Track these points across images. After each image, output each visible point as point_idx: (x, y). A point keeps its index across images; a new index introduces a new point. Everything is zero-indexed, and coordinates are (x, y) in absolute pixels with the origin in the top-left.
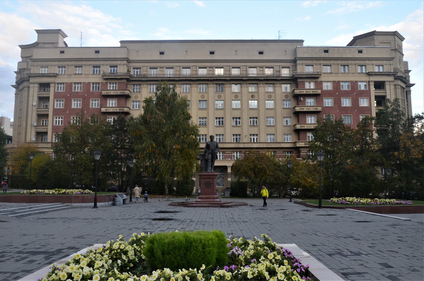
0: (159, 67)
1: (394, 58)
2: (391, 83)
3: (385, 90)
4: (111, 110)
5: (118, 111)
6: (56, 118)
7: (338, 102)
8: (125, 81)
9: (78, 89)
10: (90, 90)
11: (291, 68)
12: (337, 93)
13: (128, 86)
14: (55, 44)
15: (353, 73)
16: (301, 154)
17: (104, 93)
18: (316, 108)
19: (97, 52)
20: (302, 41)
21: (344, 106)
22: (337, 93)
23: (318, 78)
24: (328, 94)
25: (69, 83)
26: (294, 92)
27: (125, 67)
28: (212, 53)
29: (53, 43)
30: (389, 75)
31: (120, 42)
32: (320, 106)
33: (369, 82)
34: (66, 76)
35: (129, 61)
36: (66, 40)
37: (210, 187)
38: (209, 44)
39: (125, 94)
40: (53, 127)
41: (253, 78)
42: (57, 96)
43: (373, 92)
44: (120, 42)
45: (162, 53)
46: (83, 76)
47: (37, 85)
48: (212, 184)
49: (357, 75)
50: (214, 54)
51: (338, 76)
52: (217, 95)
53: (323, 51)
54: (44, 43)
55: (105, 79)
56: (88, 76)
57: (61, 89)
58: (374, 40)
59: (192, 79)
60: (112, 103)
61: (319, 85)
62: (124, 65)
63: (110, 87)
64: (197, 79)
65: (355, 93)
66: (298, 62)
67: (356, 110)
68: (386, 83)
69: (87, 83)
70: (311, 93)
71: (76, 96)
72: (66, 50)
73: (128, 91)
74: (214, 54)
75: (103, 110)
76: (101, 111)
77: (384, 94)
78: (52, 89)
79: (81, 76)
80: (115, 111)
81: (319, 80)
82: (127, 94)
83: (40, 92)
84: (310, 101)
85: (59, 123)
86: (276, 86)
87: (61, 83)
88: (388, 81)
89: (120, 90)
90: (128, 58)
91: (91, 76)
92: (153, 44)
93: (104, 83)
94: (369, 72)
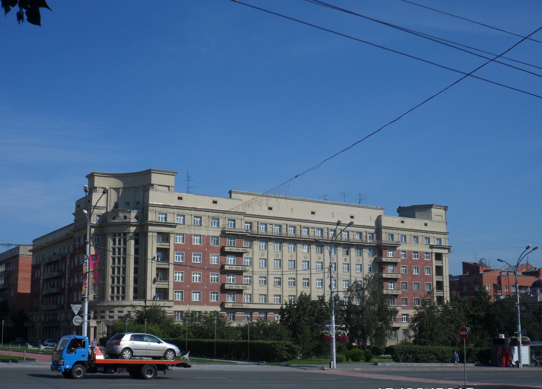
1: (449, 233)
2: (447, 255)
5: (234, 269)
18: (397, 275)
30: (445, 248)
40: (174, 283)
42: (177, 248)
43: (435, 263)
47: (156, 234)
49: (424, 245)
54: (159, 185)
58: (432, 212)
64: (304, 239)
69: (206, 236)
71: (196, 249)
78: (172, 240)
81: (398, 248)
83: (163, 243)
84: (390, 268)
87: (180, 234)
91: (210, 228)
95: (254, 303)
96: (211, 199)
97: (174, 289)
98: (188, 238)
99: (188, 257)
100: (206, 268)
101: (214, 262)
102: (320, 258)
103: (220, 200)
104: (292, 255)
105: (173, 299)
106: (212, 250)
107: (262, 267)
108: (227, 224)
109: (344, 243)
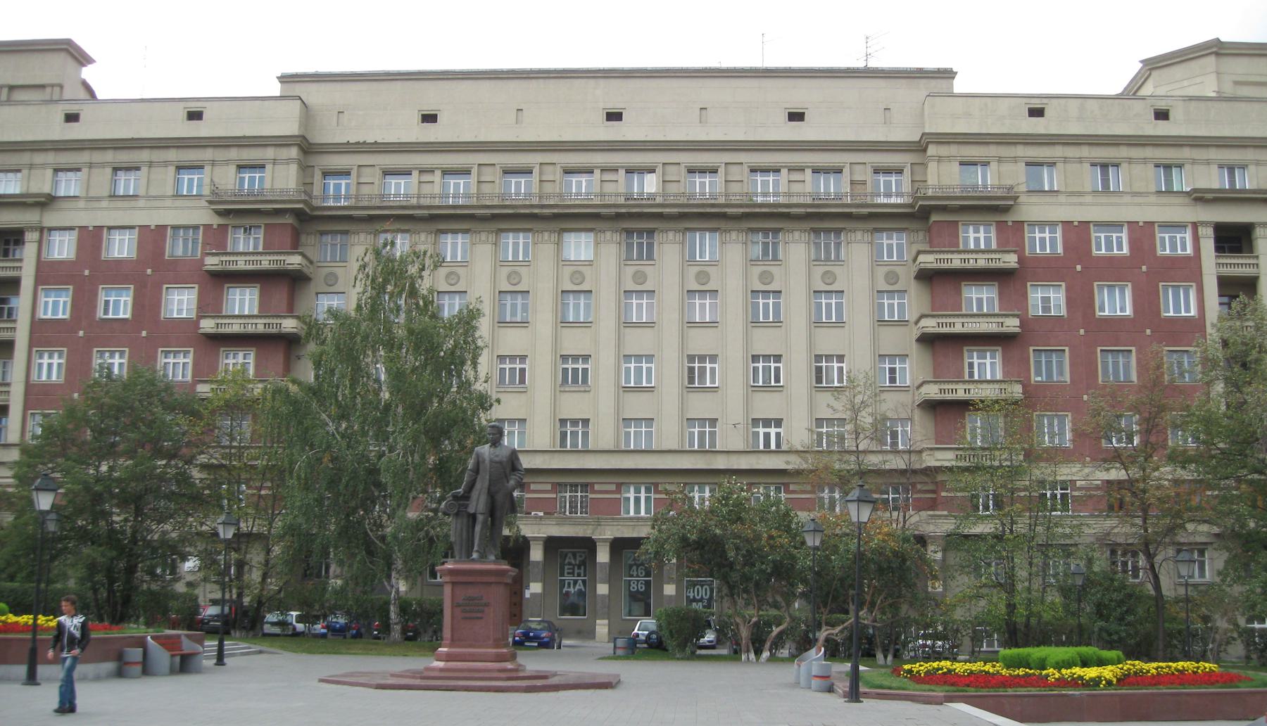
0: (416, 169)
3: (1254, 257)
4: (236, 328)
7: (1081, 301)
8: (289, 220)
9: (121, 247)
10: (163, 254)
11: (907, 171)
12: (1079, 268)
13: (303, 238)
14: (48, 90)
17: (212, 262)
18: (1000, 320)
19: (195, 116)
20: (948, 74)
21: (1106, 313)
22: (1079, 268)
23: (1006, 210)
24: (1047, 270)
25: (91, 228)
26: (917, 262)
27: (294, 168)
28: (614, 116)
29: (42, 87)
31: (278, 78)
32: (1014, 316)
33: (1195, 226)
35: (307, 148)
36: (87, 73)
37: (478, 618)
38: (602, 82)
39: (290, 267)
40: (29, 387)
41: (764, 210)
42: (49, 274)
43: (1211, 265)
44: (278, 78)
45: (429, 118)
46: (141, 203)
48: (458, 605)
49: (1153, 199)
50: (621, 120)
51: (1081, 204)
52: (630, 271)
54: (12, 88)
55: (221, 213)
57: (63, 248)
59: (536, 211)
60: (242, 302)
61: (1012, 233)
62: (289, 161)
63: (235, 240)
64: (555, 211)
65: (1144, 268)
66: (932, 150)
67: (1148, 332)
70: (982, 264)
71: (117, 273)
72: (86, 112)
73: (300, 257)
74: (621, 120)
75: (208, 325)
76: (201, 331)
78: (29, 252)
79: (133, 204)
80: (250, 329)
81: (1010, 218)
82: (297, 267)
84: (980, 296)
86: (853, 239)
89: (270, 254)
90: (304, 137)
91: (168, 203)
92: (399, 84)
93: (215, 227)
94: (1195, 191)
98: (91, 238)
101: (180, 311)
106: (178, 273)
109: (742, 210)
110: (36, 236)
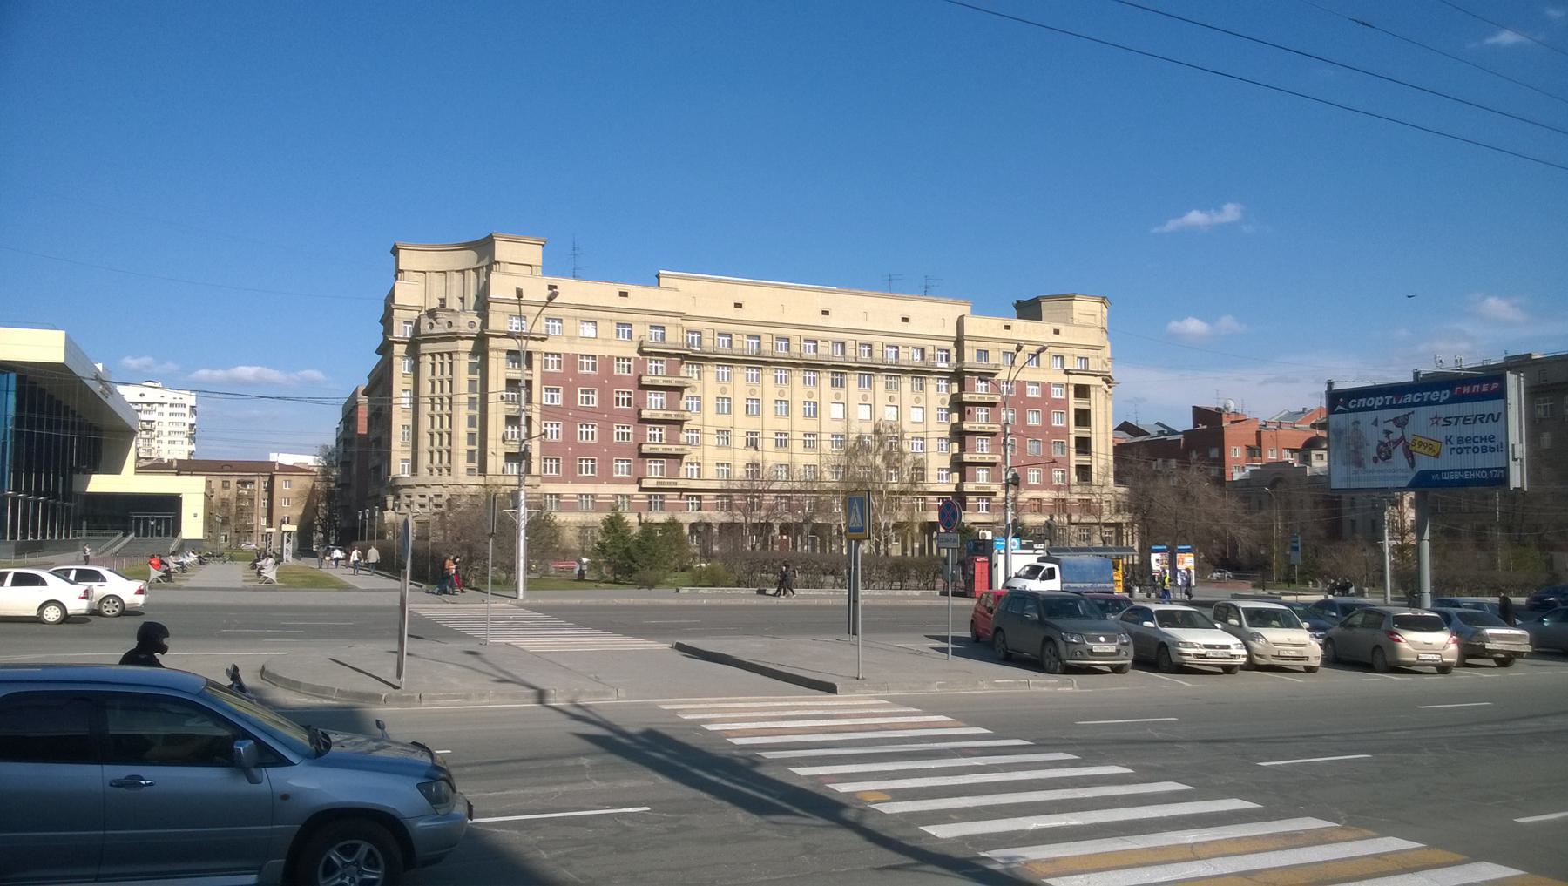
6: (581, 426)
15: (1045, 369)
16: (968, 503)
23: (993, 375)
33: (1067, 384)
34: (565, 340)
43: (1074, 403)
46: (599, 342)
47: (504, 354)
53: (1003, 327)
56: (609, 343)
58: (1072, 308)
68: (1091, 388)
77: (1087, 407)
78: (536, 364)
81: (996, 377)
84: (981, 413)
85: (587, 438)
88: (1093, 386)
91: (614, 343)
95: (707, 478)
96: (616, 288)
97: (541, 454)
98: (571, 361)
99: (570, 397)
100: (603, 416)
102: (840, 396)
103: (631, 289)
104: (752, 389)
105: (540, 472)
107: (723, 413)
108: (648, 335)
110: (539, 356)
